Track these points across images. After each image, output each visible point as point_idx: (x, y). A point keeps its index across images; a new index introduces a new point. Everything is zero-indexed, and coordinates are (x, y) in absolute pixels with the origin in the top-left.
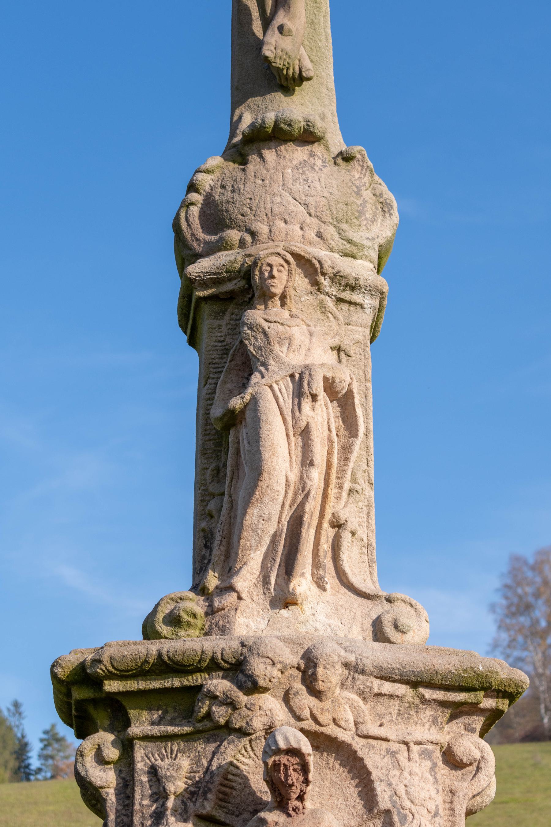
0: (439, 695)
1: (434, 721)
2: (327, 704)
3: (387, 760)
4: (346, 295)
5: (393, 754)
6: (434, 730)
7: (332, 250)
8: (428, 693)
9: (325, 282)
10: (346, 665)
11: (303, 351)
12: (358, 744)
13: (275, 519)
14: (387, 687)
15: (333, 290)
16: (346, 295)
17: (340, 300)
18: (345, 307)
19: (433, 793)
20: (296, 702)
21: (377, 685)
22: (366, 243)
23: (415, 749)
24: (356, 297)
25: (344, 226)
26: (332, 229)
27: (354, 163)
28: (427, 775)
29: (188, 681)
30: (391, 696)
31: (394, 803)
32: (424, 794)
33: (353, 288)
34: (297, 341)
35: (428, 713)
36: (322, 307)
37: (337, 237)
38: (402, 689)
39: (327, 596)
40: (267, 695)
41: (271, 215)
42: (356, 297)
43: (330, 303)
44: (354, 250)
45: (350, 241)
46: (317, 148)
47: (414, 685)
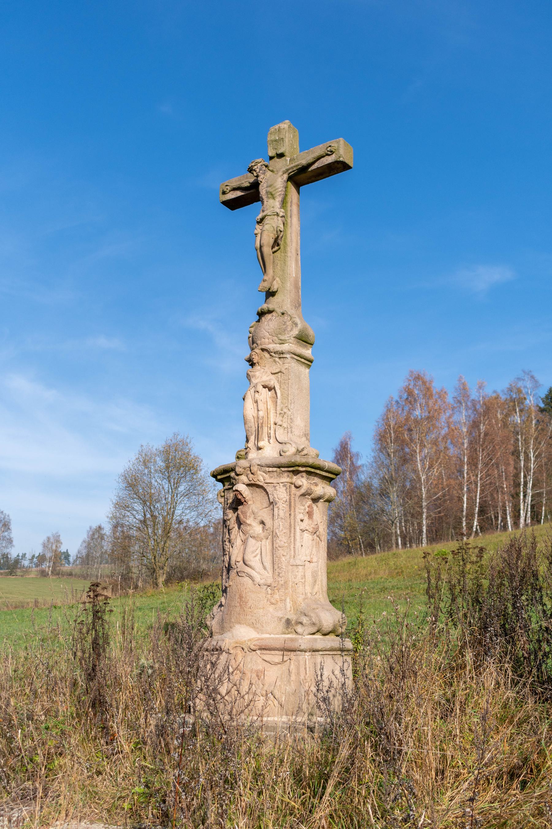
0: (286, 469)
1: (288, 476)
2: (256, 476)
3: (273, 489)
4: (281, 356)
5: (275, 487)
6: (288, 479)
7: (276, 344)
8: (283, 469)
9: (272, 354)
10: (258, 465)
11: (259, 378)
12: (265, 486)
13: (253, 427)
14: (271, 469)
15: (277, 356)
16: (281, 356)
17: (280, 358)
18: (282, 359)
19: (286, 496)
20: (249, 476)
21: (267, 469)
22: (287, 338)
23: (281, 485)
24: (284, 356)
25: (279, 336)
26: (275, 338)
27: (285, 315)
28: (284, 491)
29: (228, 475)
30: (273, 471)
31: (274, 500)
32: (282, 497)
33: (282, 354)
34: (257, 376)
35: (286, 474)
36: (275, 361)
37: (277, 339)
38: (275, 469)
39: (271, 445)
40: (243, 476)
41: (261, 338)
42: (284, 356)
43: (277, 359)
44: (283, 342)
45: (281, 340)
46: (274, 314)
47: (279, 467)
